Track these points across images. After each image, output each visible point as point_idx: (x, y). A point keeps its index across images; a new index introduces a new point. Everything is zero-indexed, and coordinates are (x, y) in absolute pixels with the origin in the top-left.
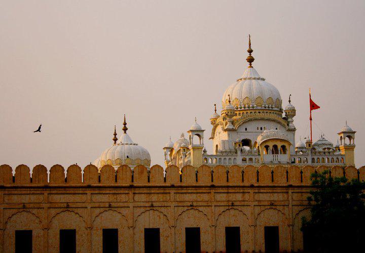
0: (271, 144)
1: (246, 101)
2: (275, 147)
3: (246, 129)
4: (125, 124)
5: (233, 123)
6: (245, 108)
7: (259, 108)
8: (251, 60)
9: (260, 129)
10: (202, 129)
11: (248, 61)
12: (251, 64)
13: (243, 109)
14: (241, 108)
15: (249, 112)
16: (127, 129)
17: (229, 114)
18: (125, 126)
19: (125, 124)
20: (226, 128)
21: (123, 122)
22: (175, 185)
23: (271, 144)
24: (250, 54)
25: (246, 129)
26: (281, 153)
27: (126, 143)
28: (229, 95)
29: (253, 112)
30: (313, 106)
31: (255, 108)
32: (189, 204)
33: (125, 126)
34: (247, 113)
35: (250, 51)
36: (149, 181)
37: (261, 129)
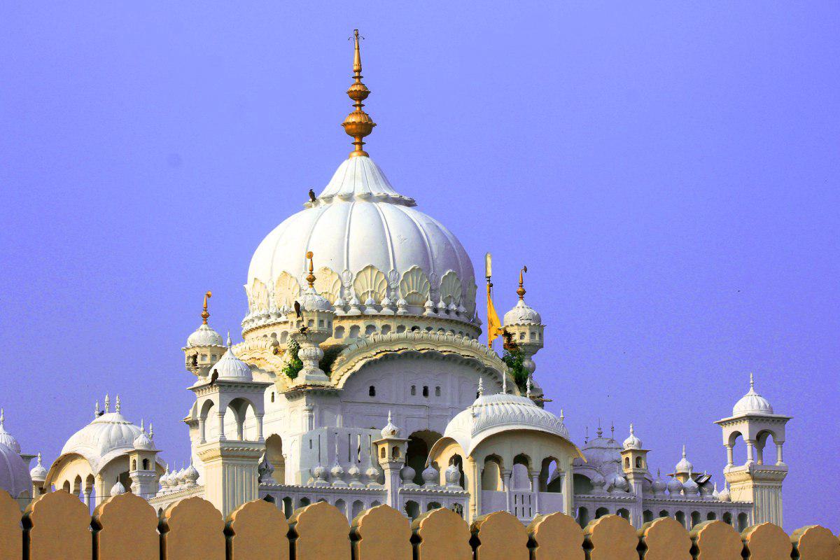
0: (507, 452)
1: (365, 284)
3: (372, 392)
7: (417, 311)
8: (363, 130)
9: (420, 390)
11: (349, 132)
13: (354, 311)
15: (379, 324)
17: (315, 327)
23: (507, 452)
25: (372, 392)
28: (310, 255)
29: (394, 325)
31: (401, 311)
35: (361, 96)
37: (426, 392)
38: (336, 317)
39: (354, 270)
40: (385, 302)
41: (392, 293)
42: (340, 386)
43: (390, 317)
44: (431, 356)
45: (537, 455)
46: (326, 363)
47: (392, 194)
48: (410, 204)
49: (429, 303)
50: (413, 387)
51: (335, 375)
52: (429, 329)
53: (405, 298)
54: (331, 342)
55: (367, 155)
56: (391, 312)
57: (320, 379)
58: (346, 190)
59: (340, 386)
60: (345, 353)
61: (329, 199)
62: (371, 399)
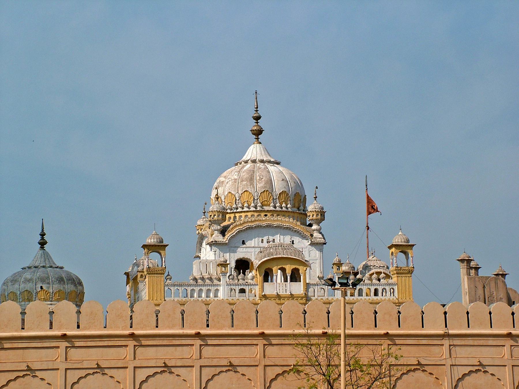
2: (283, 270)
4: (43, 235)
5: (223, 232)
6: (243, 208)
7: (266, 208)
8: (258, 133)
10: (165, 243)
12: (258, 139)
14: (237, 209)
16: (46, 243)
18: (42, 238)
19: (43, 235)
20: (211, 240)
21: (40, 231)
22: (68, 333)
24: (257, 123)
25: (244, 243)
26: (291, 281)
27: (42, 265)
29: (256, 214)
30: (372, 208)
32: (225, 362)
33: (42, 238)
34: (246, 216)
35: (257, 118)
36: (51, 328)
38: (228, 213)
39: (240, 192)
40: (253, 205)
41: (256, 201)
42: (227, 242)
43: (254, 211)
44: (269, 226)
45: (289, 268)
46: (223, 232)
47: (272, 160)
48: (278, 163)
49: (272, 204)
50: (262, 240)
51: (226, 237)
52: (278, 215)
53: (261, 203)
54: (226, 223)
55: (260, 143)
56: (254, 209)
57: (220, 238)
58: (254, 158)
59: (227, 242)
60: (231, 226)
61: (246, 162)
62: (244, 246)
